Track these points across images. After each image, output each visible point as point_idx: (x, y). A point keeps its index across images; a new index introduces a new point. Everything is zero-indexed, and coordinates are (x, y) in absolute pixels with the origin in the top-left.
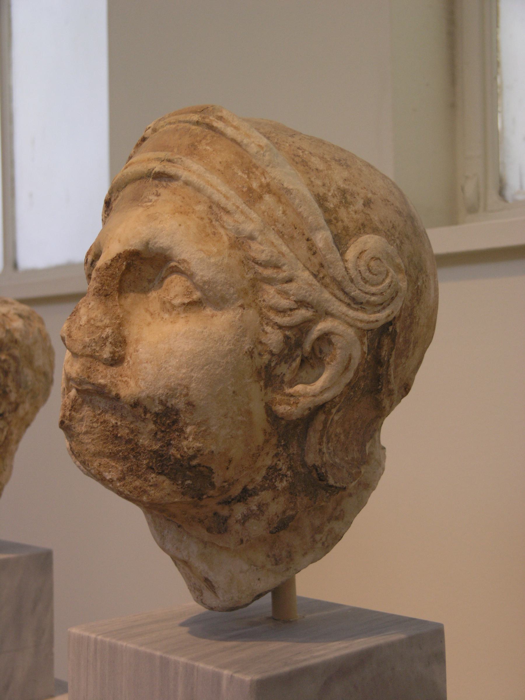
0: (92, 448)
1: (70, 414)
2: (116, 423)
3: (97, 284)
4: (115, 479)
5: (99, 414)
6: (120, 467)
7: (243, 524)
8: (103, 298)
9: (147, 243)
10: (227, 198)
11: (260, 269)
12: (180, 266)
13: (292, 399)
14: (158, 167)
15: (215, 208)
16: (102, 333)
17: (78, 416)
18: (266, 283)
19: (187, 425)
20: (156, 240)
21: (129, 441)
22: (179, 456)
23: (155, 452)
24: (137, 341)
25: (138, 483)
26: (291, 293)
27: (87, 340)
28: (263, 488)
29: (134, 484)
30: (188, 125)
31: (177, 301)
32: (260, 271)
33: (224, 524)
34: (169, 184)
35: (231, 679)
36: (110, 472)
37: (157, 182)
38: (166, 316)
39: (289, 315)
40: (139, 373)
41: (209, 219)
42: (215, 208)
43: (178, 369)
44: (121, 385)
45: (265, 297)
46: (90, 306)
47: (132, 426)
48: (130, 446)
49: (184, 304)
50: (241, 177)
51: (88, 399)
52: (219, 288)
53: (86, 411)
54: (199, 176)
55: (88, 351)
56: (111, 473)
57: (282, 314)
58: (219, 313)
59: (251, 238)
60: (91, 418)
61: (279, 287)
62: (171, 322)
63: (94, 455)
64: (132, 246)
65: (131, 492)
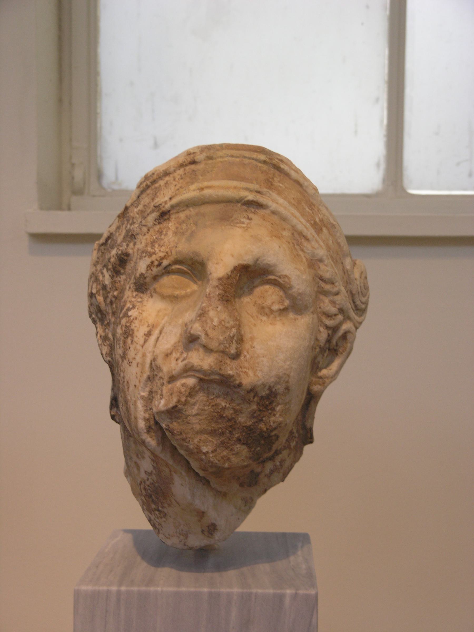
0: (197, 427)
1: (186, 400)
2: (226, 406)
3: (221, 291)
4: (210, 452)
5: (212, 399)
6: (215, 441)
7: (270, 477)
8: (225, 302)
9: (257, 260)
10: (307, 228)
11: (323, 284)
12: (279, 280)
13: (321, 380)
14: (251, 197)
15: (296, 234)
16: (230, 333)
17: (192, 401)
18: (323, 295)
19: (279, 404)
20: (265, 258)
21: (230, 420)
22: (265, 429)
23: (248, 427)
24: (252, 339)
25: (225, 453)
26: (337, 302)
27: (221, 338)
28: (285, 448)
29: (222, 455)
30: (254, 162)
31: (276, 307)
32: (323, 286)
33: (255, 478)
34: (257, 210)
35: (295, 596)
36: (207, 445)
37: (245, 207)
38: (265, 318)
39: (334, 319)
40: (257, 365)
41: (293, 243)
42: (296, 234)
43: (285, 361)
44: (243, 376)
45: (322, 305)
46: (219, 309)
47: (238, 407)
48: (229, 424)
49: (280, 310)
50: (309, 212)
51: (205, 386)
52: (306, 298)
53: (201, 397)
54: (285, 208)
55: (222, 347)
56: (209, 447)
57: (330, 318)
58: (299, 317)
59: (321, 260)
60: (204, 402)
61: (331, 298)
62: (271, 324)
63: (197, 433)
64: (245, 261)
65: (219, 461)
